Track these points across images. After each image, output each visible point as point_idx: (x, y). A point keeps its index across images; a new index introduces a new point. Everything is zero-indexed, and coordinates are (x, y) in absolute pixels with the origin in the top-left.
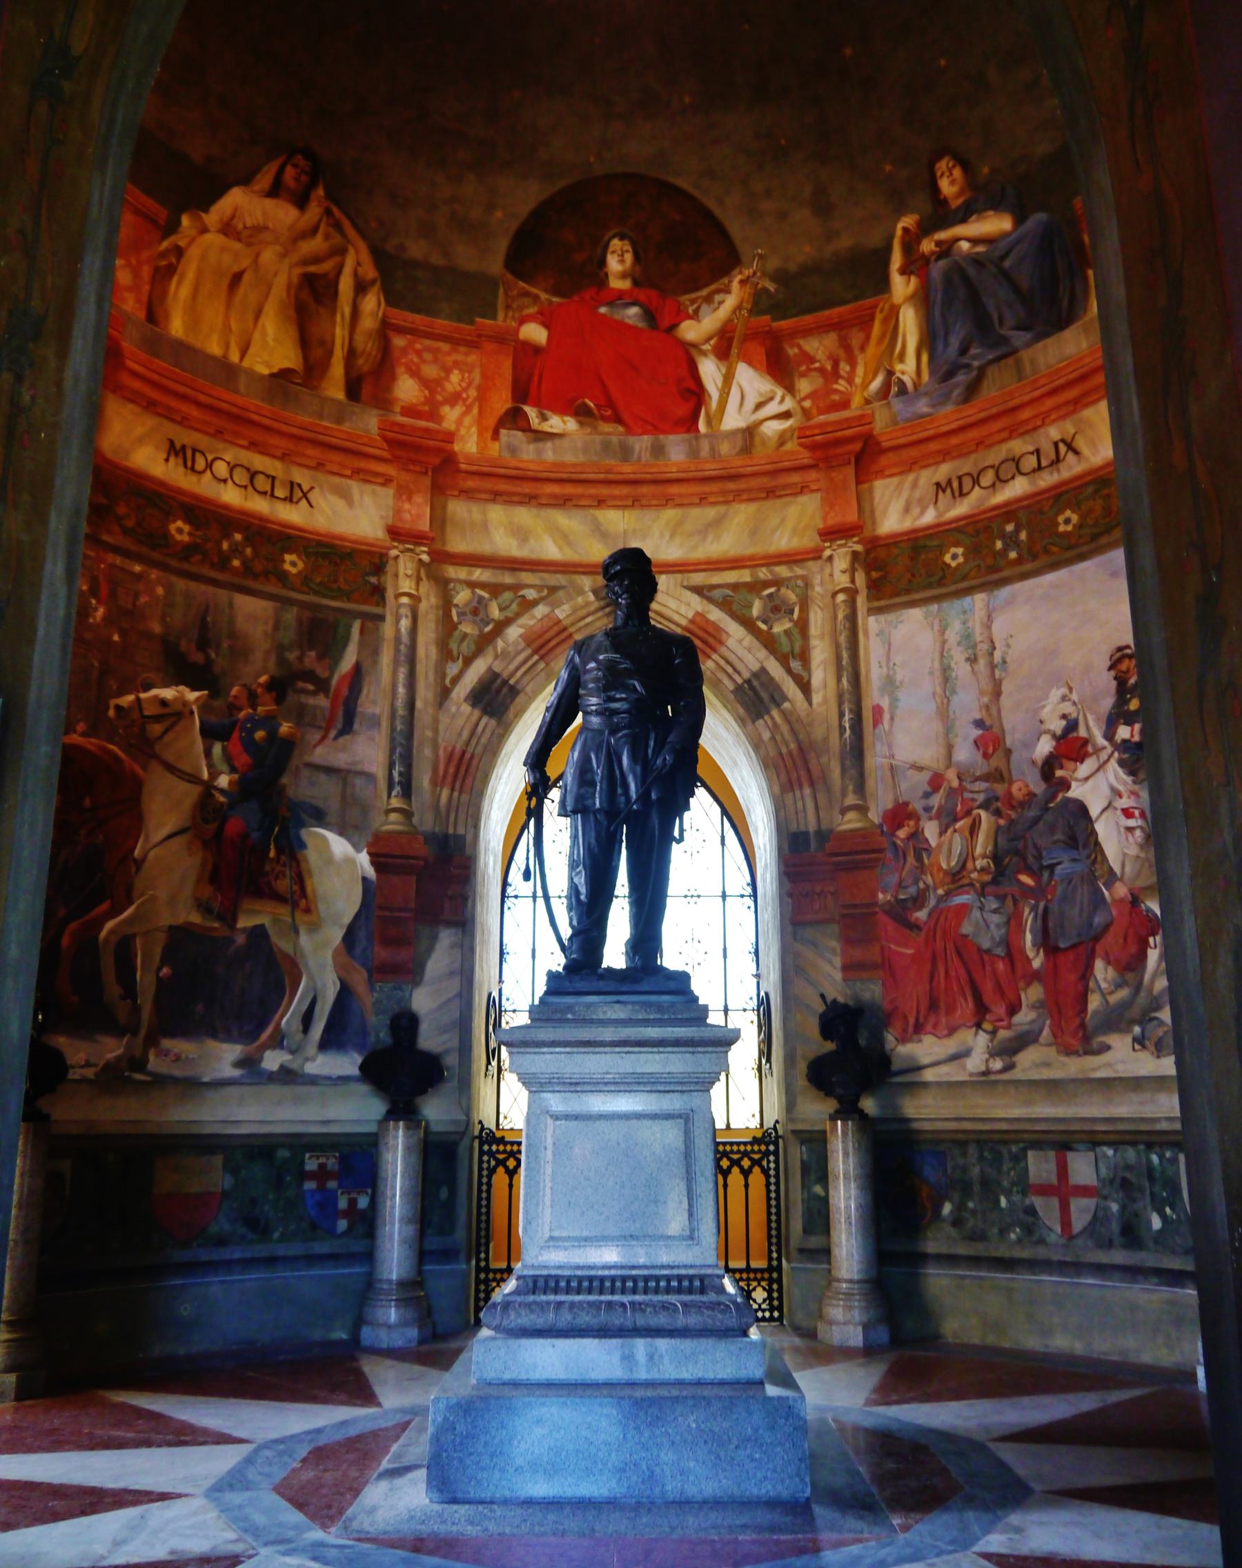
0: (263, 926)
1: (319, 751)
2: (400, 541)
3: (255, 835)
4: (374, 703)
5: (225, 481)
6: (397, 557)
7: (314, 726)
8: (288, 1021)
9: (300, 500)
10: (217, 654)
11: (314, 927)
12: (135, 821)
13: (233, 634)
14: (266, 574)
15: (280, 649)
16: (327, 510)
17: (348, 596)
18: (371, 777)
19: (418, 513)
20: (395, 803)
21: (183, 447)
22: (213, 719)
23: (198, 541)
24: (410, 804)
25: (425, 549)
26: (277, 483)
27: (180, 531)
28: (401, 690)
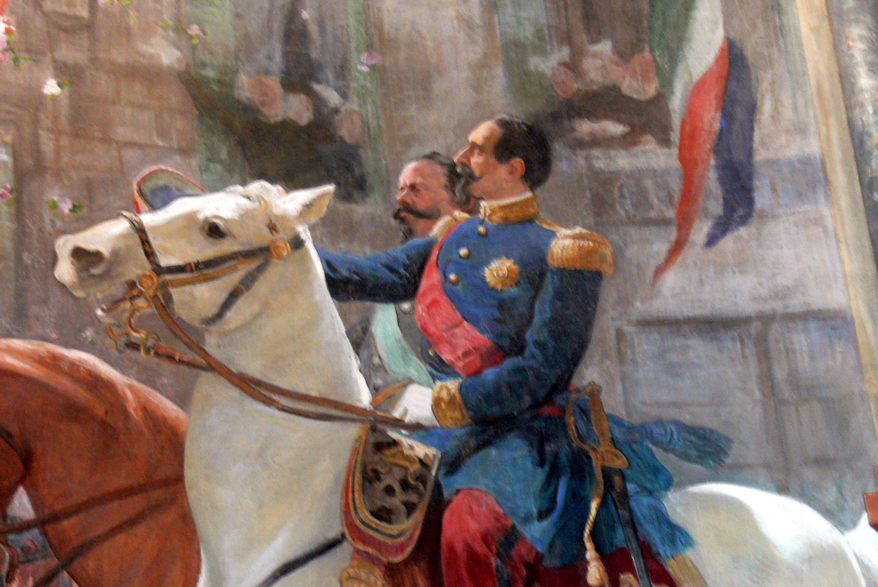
1: (671, 279)
3: (537, 533)
4: (800, 130)
7: (648, 223)
10: (344, 95)
13: (377, 40)
15: (514, 53)
18: (833, 322)
22: (362, 254)
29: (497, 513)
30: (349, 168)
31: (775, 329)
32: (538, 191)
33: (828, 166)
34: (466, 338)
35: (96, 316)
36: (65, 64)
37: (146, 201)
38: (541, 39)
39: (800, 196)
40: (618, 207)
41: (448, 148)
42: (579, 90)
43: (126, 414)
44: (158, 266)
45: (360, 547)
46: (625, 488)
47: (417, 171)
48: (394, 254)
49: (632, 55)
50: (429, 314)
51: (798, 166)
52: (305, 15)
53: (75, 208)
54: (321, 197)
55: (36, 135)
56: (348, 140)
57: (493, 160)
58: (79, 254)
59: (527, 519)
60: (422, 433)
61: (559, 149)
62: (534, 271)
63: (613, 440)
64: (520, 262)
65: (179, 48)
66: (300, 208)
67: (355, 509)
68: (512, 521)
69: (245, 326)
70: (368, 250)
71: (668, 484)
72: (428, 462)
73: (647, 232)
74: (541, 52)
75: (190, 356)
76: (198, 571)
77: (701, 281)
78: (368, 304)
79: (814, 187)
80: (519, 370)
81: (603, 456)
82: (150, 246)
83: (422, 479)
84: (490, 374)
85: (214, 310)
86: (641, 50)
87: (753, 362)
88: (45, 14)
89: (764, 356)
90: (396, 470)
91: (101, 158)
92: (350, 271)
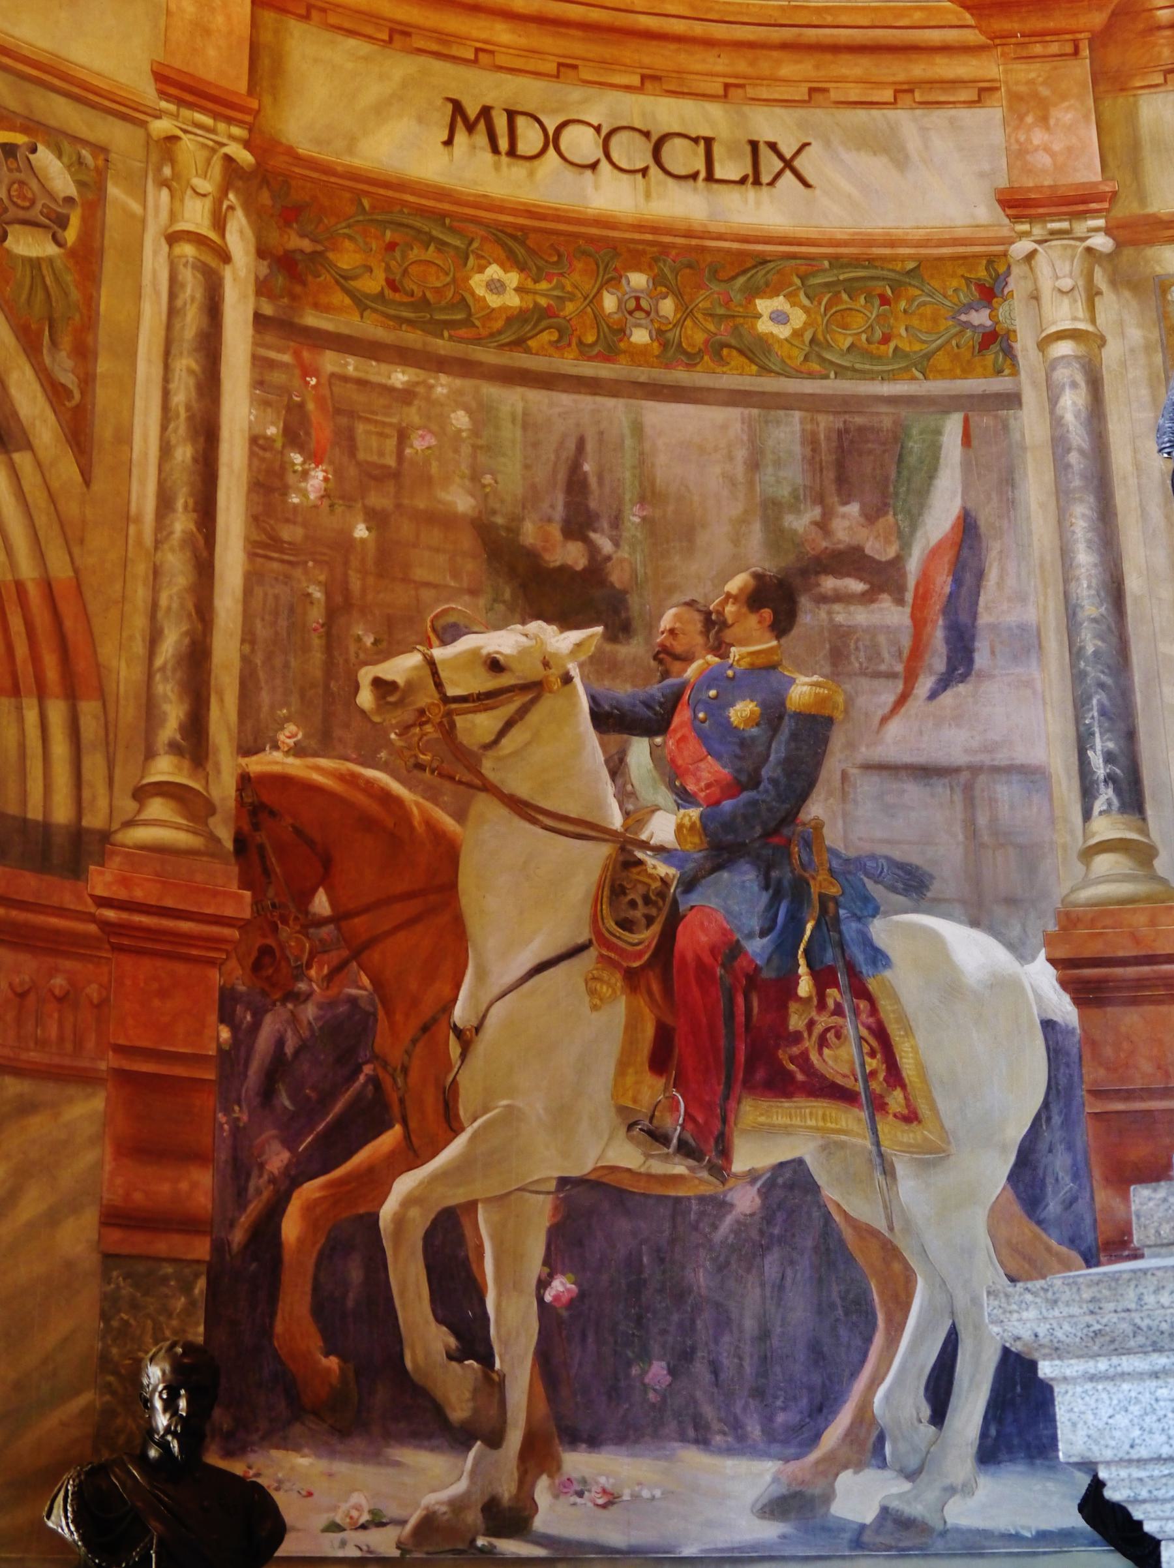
0: (799, 1163)
1: (894, 728)
2: (1031, 219)
4: (1021, 598)
5: (594, 166)
6: (1031, 255)
7: (877, 675)
8: (887, 1397)
9: (778, 175)
10: (617, 544)
11: (933, 1156)
12: (452, 946)
13: (649, 495)
14: (716, 350)
15: (771, 511)
16: (846, 186)
17: (924, 365)
18: (1032, 776)
19: (1068, 146)
20: (1105, 828)
21: (486, 112)
22: (623, 691)
23: (543, 302)
24: (1144, 831)
25: (1101, 222)
26: (717, 149)
27: (496, 287)
28: (1085, 558)
29: (725, 929)
30: (616, 612)
31: (982, 778)
32: (783, 641)
33: (1042, 634)
34: (711, 770)
35: (390, 740)
36: (373, 510)
37: (438, 637)
38: (797, 498)
39: (1015, 659)
40: (853, 658)
41: (706, 595)
42: (826, 548)
43: (412, 828)
44: (445, 695)
45: (605, 952)
46: (838, 913)
47: (677, 617)
48: (651, 692)
49: (878, 517)
50: (678, 747)
51: (1016, 631)
52: (586, 467)
53: (376, 642)
54: (591, 636)
55: (346, 575)
56: (617, 585)
57: (744, 610)
58: (378, 683)
59: (750, 936)
60: (665, 855)
61: (805, 602)
62: (774, 714)
63: (831, 870)
64: (763, 705)
65: (473, 495)
66: (571, 646)
67: (602, 919)
68: (738, 936)
69: (515, 753)
70: (629, 689)
71: (875, 912)
72: (669, 881)
73: (877, 683)
74: (795, 509)
75: (468, 777)
76: (466, 966)
77: (921, 733)
78: (625, 736)
79: (1029, 650)
80: (754, 803)
81: (821, 884)
82: (439, 677)
83: (662, 895)
84: (727, 805)
85: (493, 737)
86: (886, 513)
87: (959, 806)
88: (359, 464)
89: (970, 802)
90: (639, 886)
91: (400, 596)
92: (611, 705)
